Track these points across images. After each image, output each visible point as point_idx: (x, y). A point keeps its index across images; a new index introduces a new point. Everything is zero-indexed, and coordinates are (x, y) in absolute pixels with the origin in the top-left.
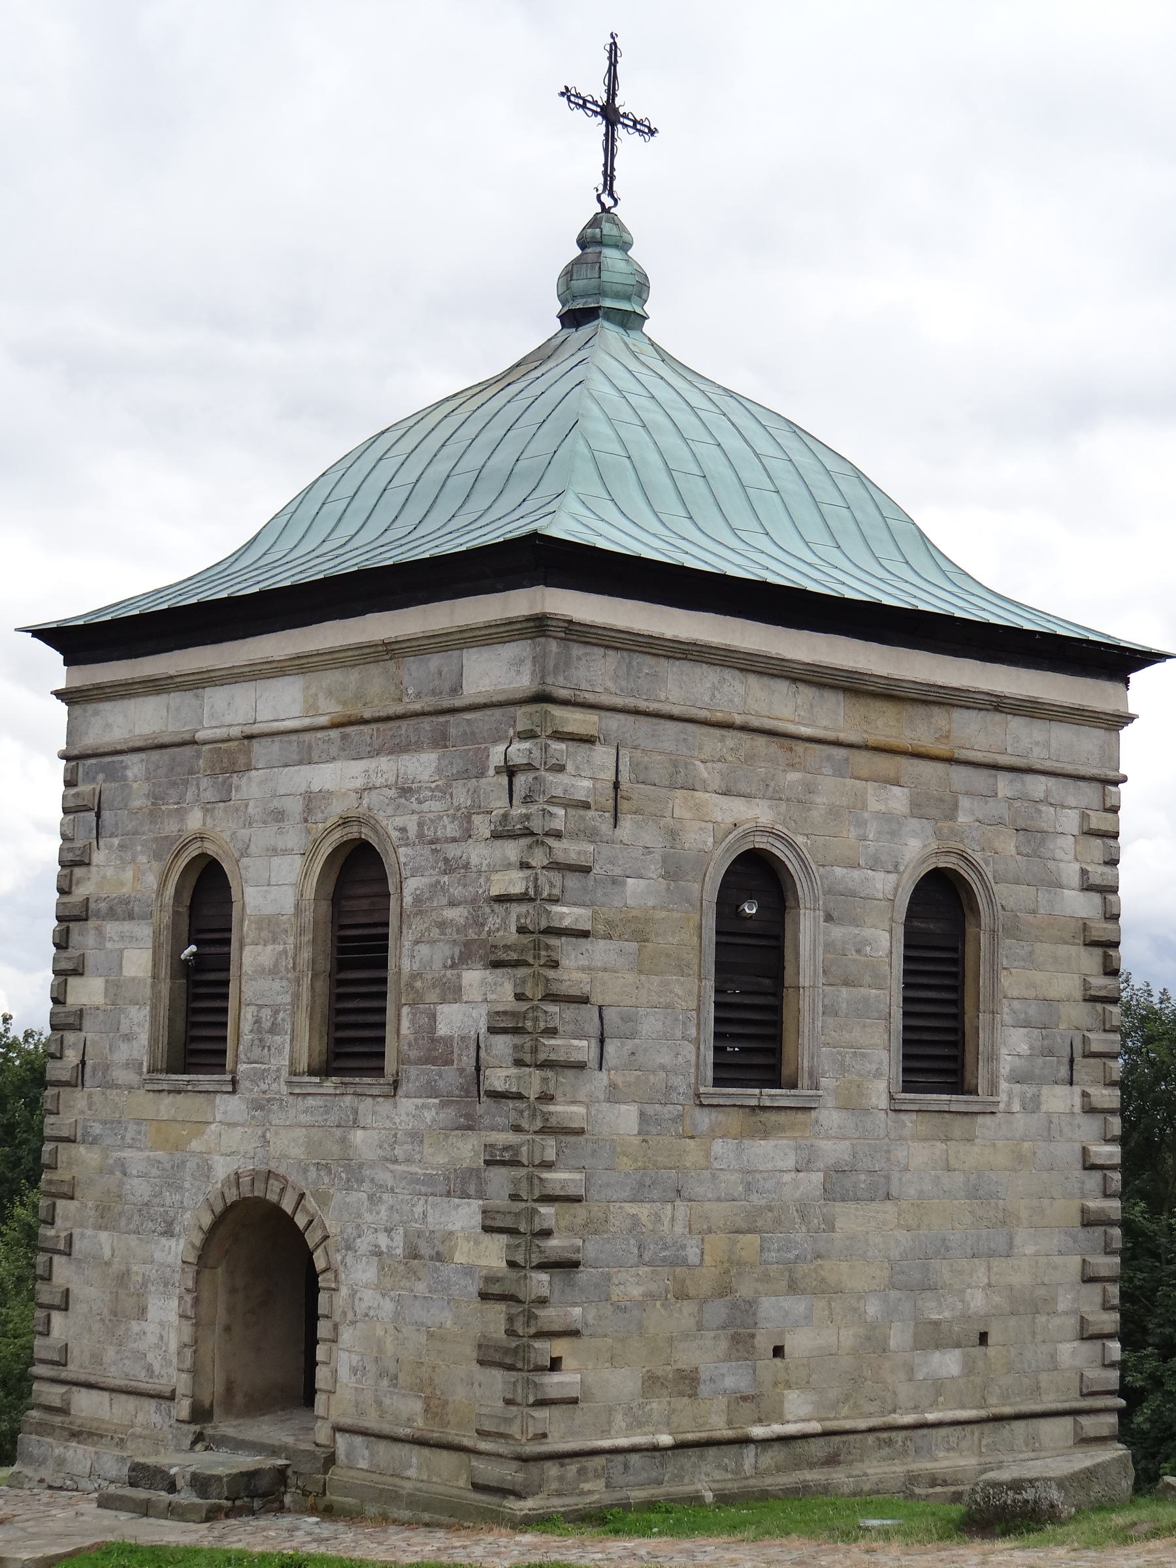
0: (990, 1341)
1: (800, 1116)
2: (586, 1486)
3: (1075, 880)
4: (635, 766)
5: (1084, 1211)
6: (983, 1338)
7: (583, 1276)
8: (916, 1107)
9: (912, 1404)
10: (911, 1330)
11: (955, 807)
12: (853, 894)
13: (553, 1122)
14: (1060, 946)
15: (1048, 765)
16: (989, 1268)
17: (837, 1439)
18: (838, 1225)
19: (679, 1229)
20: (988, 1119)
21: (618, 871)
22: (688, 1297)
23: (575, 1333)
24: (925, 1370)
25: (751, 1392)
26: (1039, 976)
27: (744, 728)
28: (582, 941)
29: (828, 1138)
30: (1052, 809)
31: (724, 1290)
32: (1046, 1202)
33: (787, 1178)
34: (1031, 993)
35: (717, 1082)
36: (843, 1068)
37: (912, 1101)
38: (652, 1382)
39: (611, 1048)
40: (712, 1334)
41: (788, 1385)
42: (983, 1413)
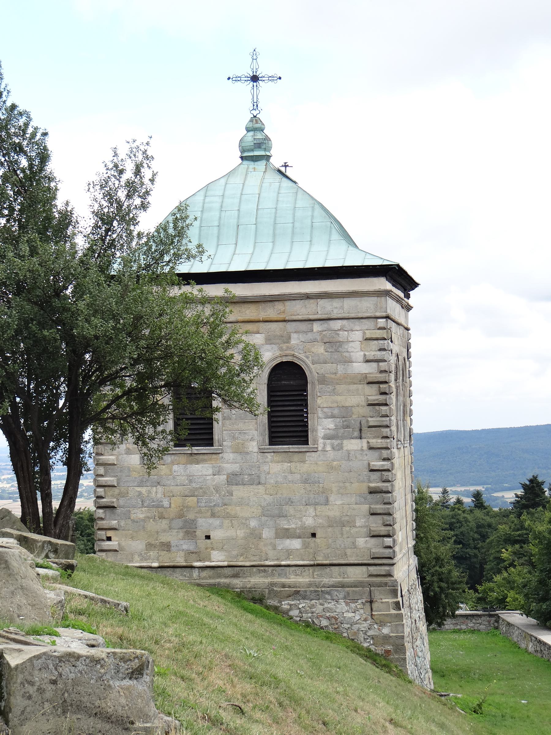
1: (214, 456)
3: (361, 359)
5: (369, 487)
6: (314, 535)
7: (119, 511)
8: (272, 451)
9: (276, 558)
10: (274, 531)
11: (290, 338)
13: (101, 462)
14: (351, 386)
15: (340, 316)
17: (238, 568)
19: (159, 495)
20: (313, 454)
22: (164, 518)
23: (115, 529)
25: (195, 551)
26: (339, 398)
29: (228, 463)
30: (346, 333)
31: (181, 516)
32: (347, 484)
33: (208, 478)
34: (335, 405)
36: (234, 438)
37: (269, 449)
38: (150, 546)
40: (176, 530)
41: (213, 549)
42: (312, 563)
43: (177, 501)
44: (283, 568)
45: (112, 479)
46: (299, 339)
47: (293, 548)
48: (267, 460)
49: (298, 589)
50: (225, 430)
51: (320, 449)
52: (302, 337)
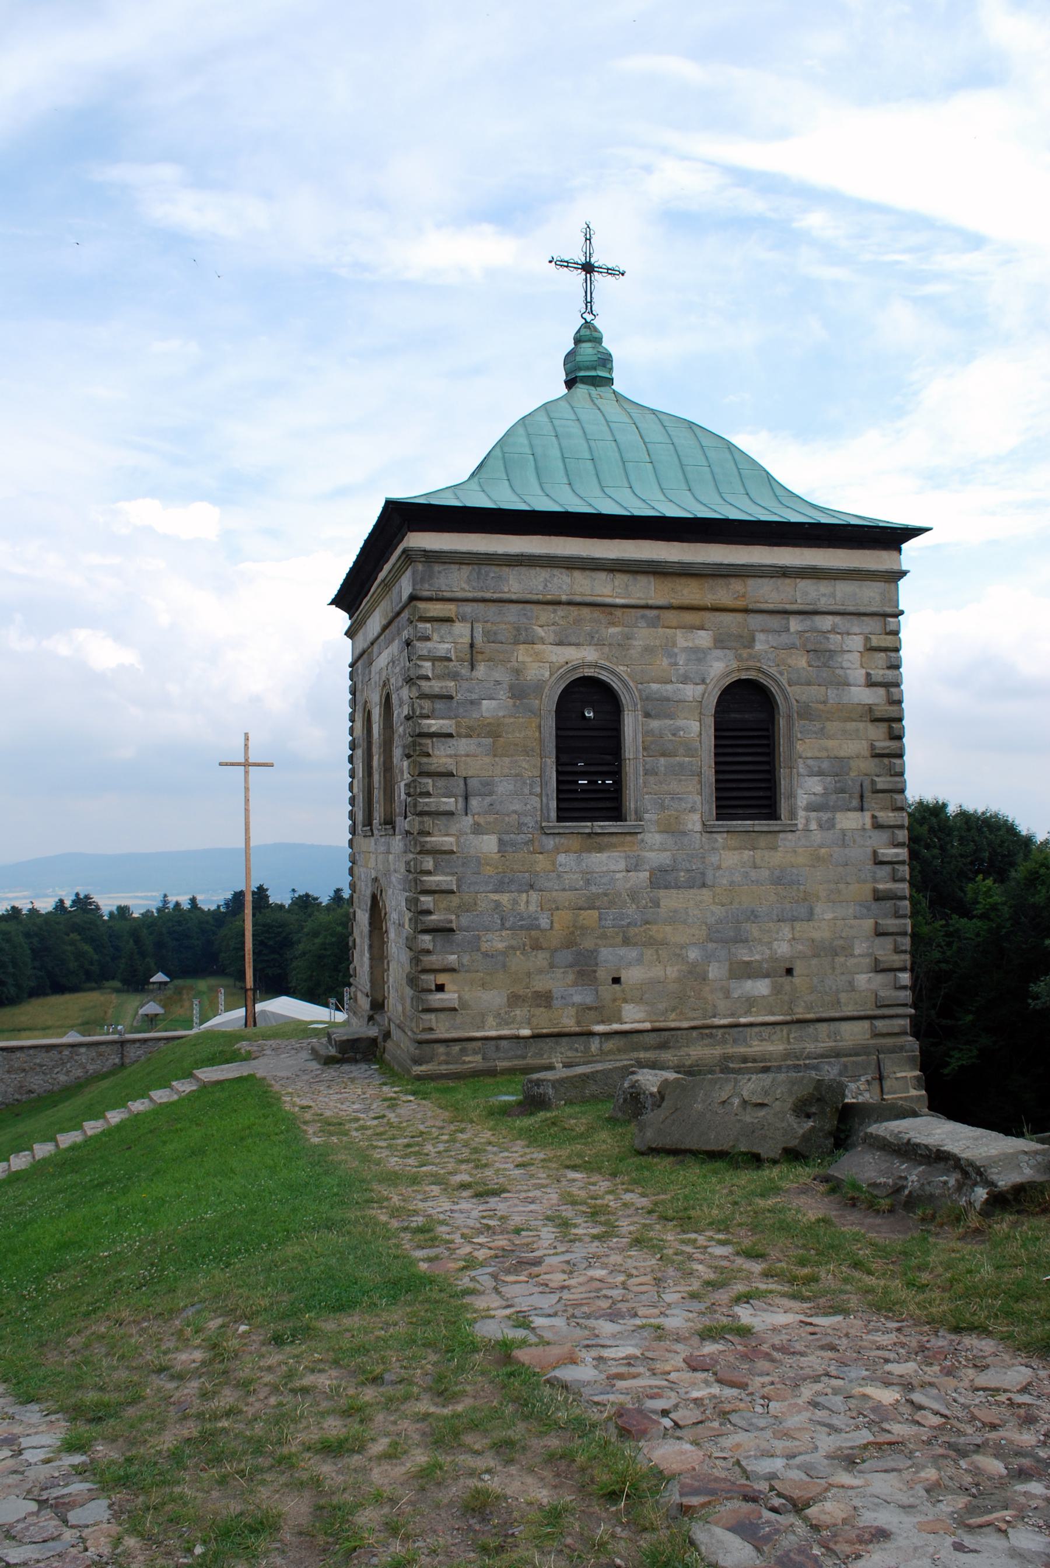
0: (795, 973)
1: (629, 838)
2: (467, 1059)
3: (862, 680)
4: (486, 633)
5: (875, 891)
6: (789, 972)
7: (459, 936)
8: (725, 829)
9: (729, 1012)
10: (727, 967)
11: (753, 640)
12: (668, 699)
13: (428, 847)
14: (848, 724)
15: (832, 608)
16: (793, 928)
17: (667, 1033)
18: (662, 904)
19: (532, 908)
20: (790, 836)
21: (474, 696)
22: (542, 948)
23: (453, 970)
24: (739, 992)
25: (595, 1005)
26: (830, 743)
27: (570, 603)
28: (449, 740)
29: (652, 850)
30: (839, 637)
31: (570, 943)
32: (842, 886)
33: (618, 876)
34: (824, 754)
35: (559, 819)
36: (663, 807)
37: (722, 826)
38: (515, 1000)
39: (474, 802)
40: (562, 970)
41: (625, 1001)
42: (788, 1018)
43: (564, 918)
44: (741, 1029)
45: (449, 878)
46: (767, 642)
47: (756, 994)
48: (717, 845)
49: (768, 1064)
50: (647, 794)
51: (800, 827)
52: (774, 641)
